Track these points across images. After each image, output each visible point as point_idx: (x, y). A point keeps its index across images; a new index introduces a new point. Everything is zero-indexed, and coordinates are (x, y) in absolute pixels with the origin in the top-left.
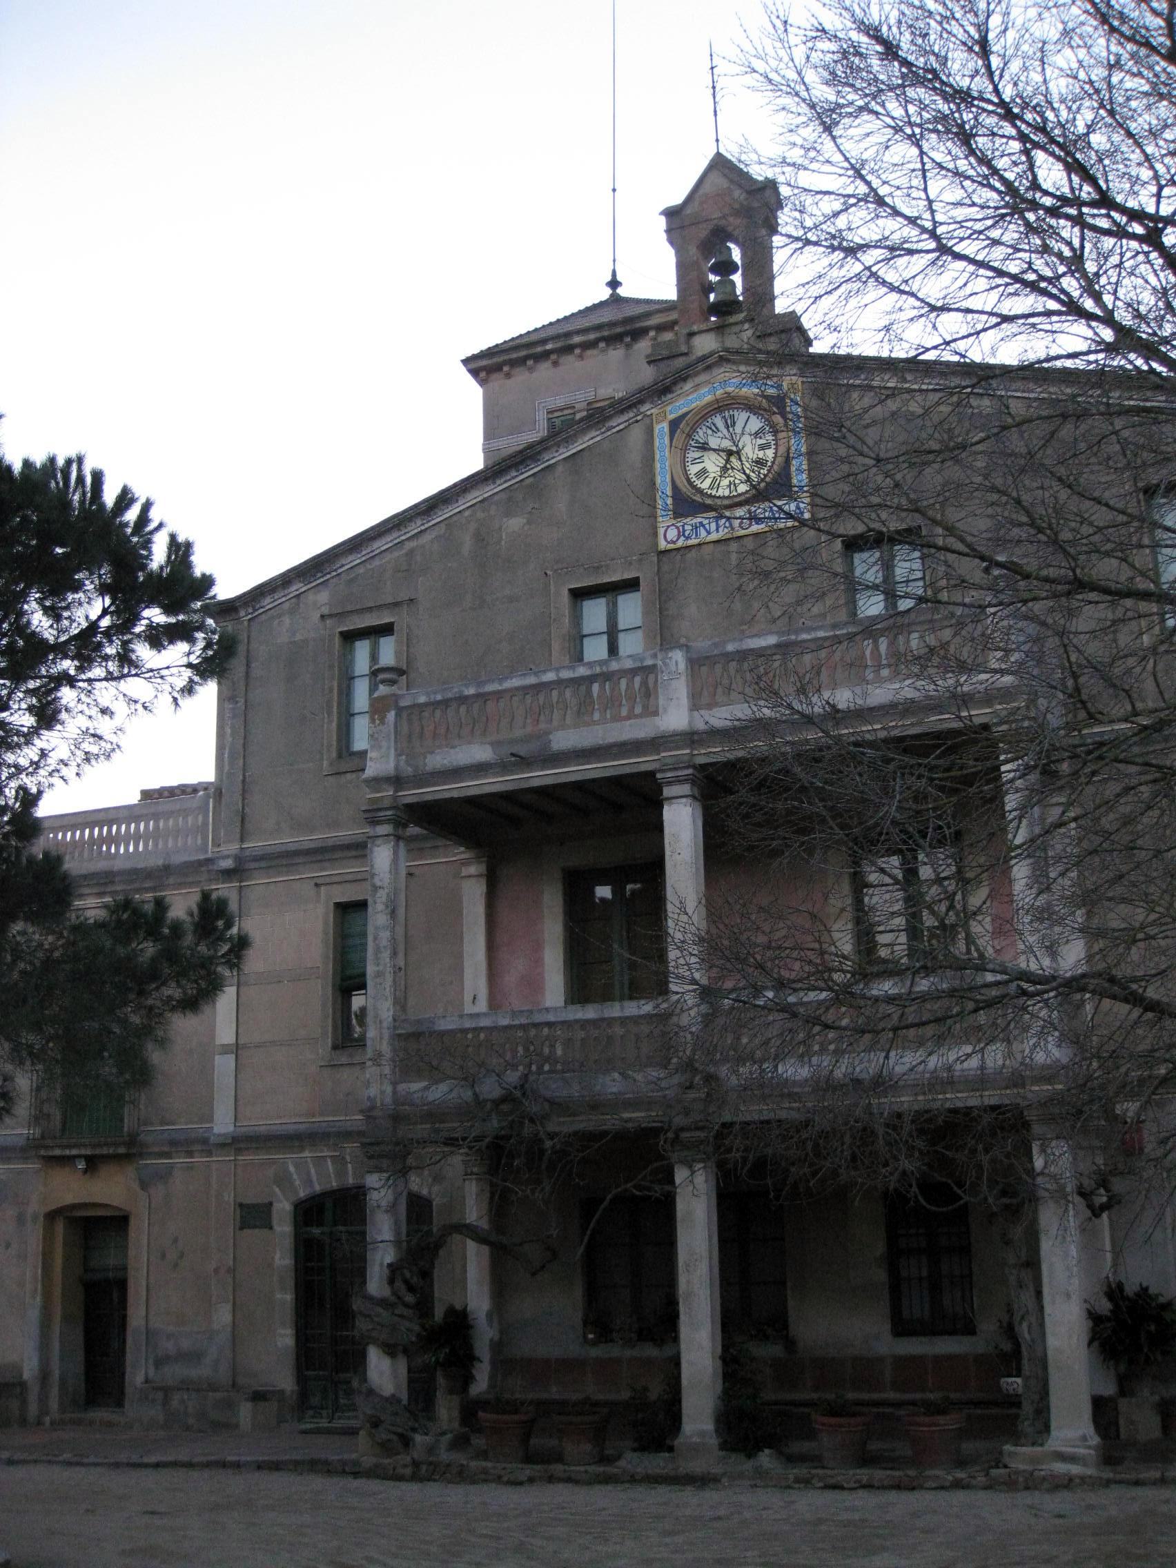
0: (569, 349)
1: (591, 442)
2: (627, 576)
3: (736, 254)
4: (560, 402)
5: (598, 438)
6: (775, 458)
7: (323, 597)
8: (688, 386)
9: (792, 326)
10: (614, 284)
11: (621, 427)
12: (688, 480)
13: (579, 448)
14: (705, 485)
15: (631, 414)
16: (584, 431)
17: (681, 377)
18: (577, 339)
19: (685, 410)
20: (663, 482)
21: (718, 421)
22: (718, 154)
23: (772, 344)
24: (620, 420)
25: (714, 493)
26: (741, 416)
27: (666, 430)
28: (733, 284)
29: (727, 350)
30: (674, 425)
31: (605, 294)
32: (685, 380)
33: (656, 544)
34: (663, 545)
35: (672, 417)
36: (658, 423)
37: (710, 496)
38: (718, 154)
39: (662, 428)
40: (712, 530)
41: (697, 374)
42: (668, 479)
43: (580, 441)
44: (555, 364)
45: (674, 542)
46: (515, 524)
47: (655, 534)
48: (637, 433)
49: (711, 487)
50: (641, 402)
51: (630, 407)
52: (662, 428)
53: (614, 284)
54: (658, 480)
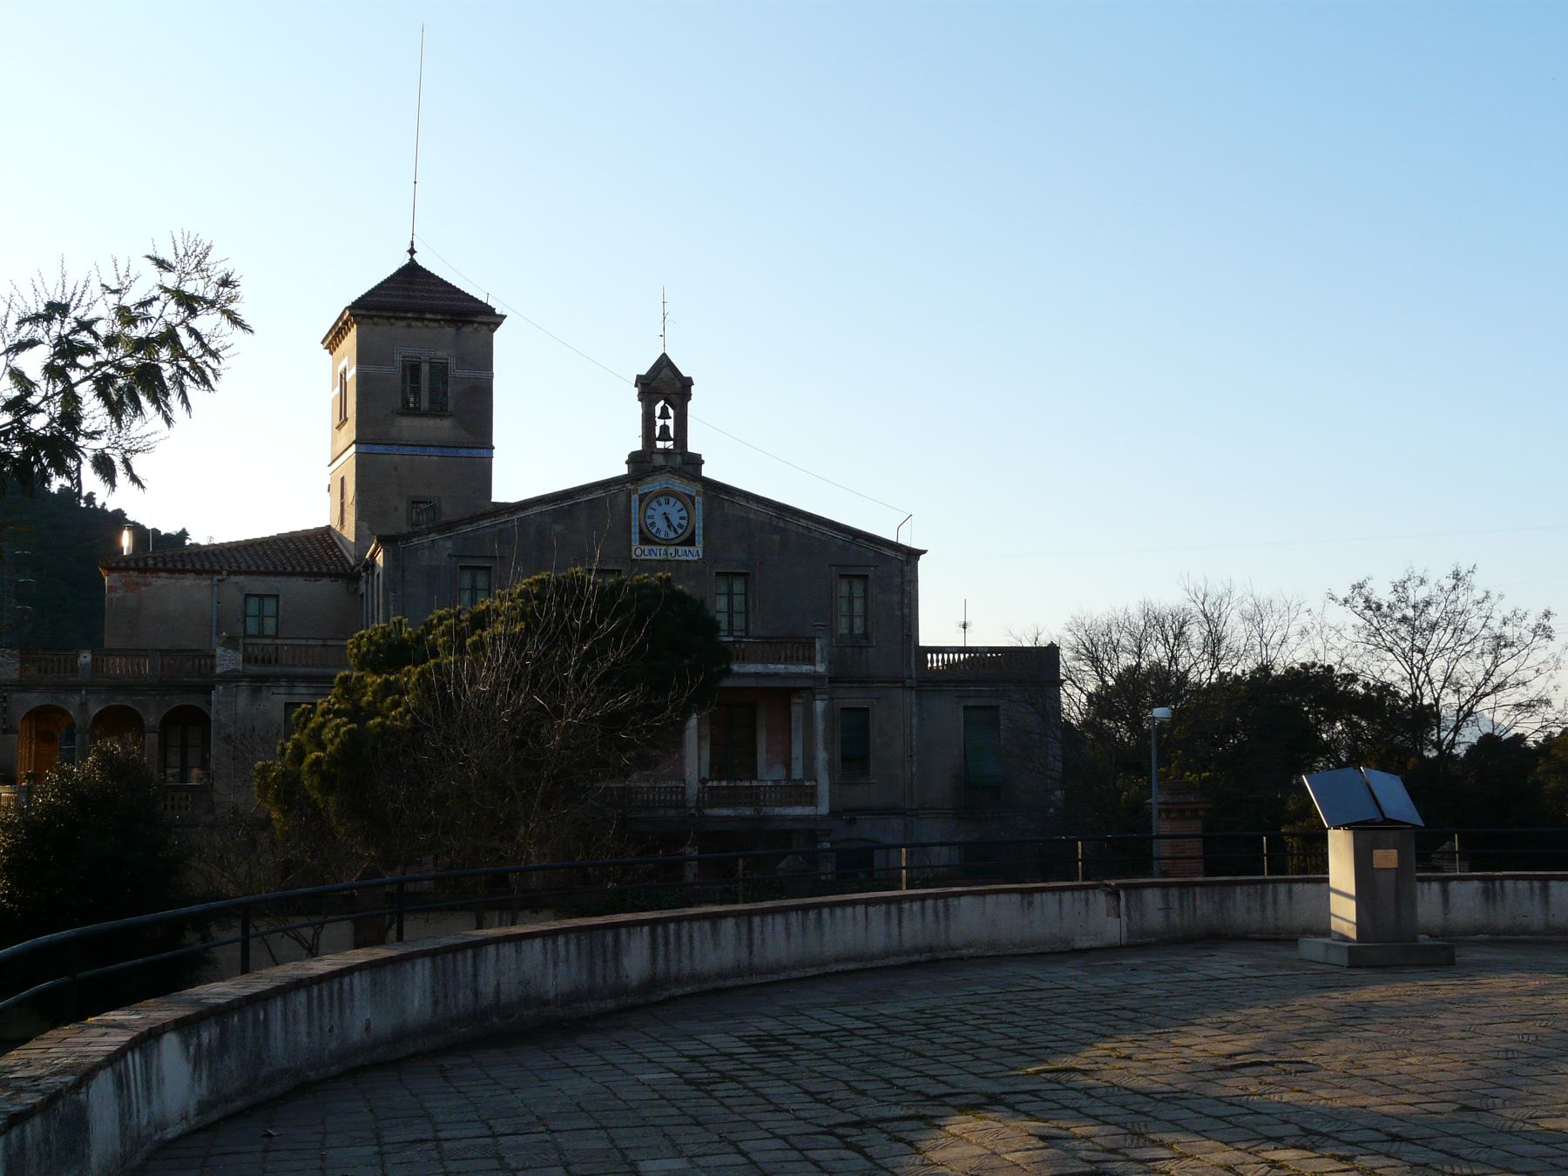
0: (422, 320)
3: (671, 412)
4: (410, 352)
7: (449, 544)
9: (697, 461)
10: (412, 252)
18: (428, 316)
20: (635, 524)
21: (662, 500)
23: (690, 469)
26: (672, 500)
31: (404, 260)
39: (635, 497)
40: (658, 553)
44: (409, 326)
46: (558, 528)
48: (622, 498)
52: (635, 497)
53: (412, 252)
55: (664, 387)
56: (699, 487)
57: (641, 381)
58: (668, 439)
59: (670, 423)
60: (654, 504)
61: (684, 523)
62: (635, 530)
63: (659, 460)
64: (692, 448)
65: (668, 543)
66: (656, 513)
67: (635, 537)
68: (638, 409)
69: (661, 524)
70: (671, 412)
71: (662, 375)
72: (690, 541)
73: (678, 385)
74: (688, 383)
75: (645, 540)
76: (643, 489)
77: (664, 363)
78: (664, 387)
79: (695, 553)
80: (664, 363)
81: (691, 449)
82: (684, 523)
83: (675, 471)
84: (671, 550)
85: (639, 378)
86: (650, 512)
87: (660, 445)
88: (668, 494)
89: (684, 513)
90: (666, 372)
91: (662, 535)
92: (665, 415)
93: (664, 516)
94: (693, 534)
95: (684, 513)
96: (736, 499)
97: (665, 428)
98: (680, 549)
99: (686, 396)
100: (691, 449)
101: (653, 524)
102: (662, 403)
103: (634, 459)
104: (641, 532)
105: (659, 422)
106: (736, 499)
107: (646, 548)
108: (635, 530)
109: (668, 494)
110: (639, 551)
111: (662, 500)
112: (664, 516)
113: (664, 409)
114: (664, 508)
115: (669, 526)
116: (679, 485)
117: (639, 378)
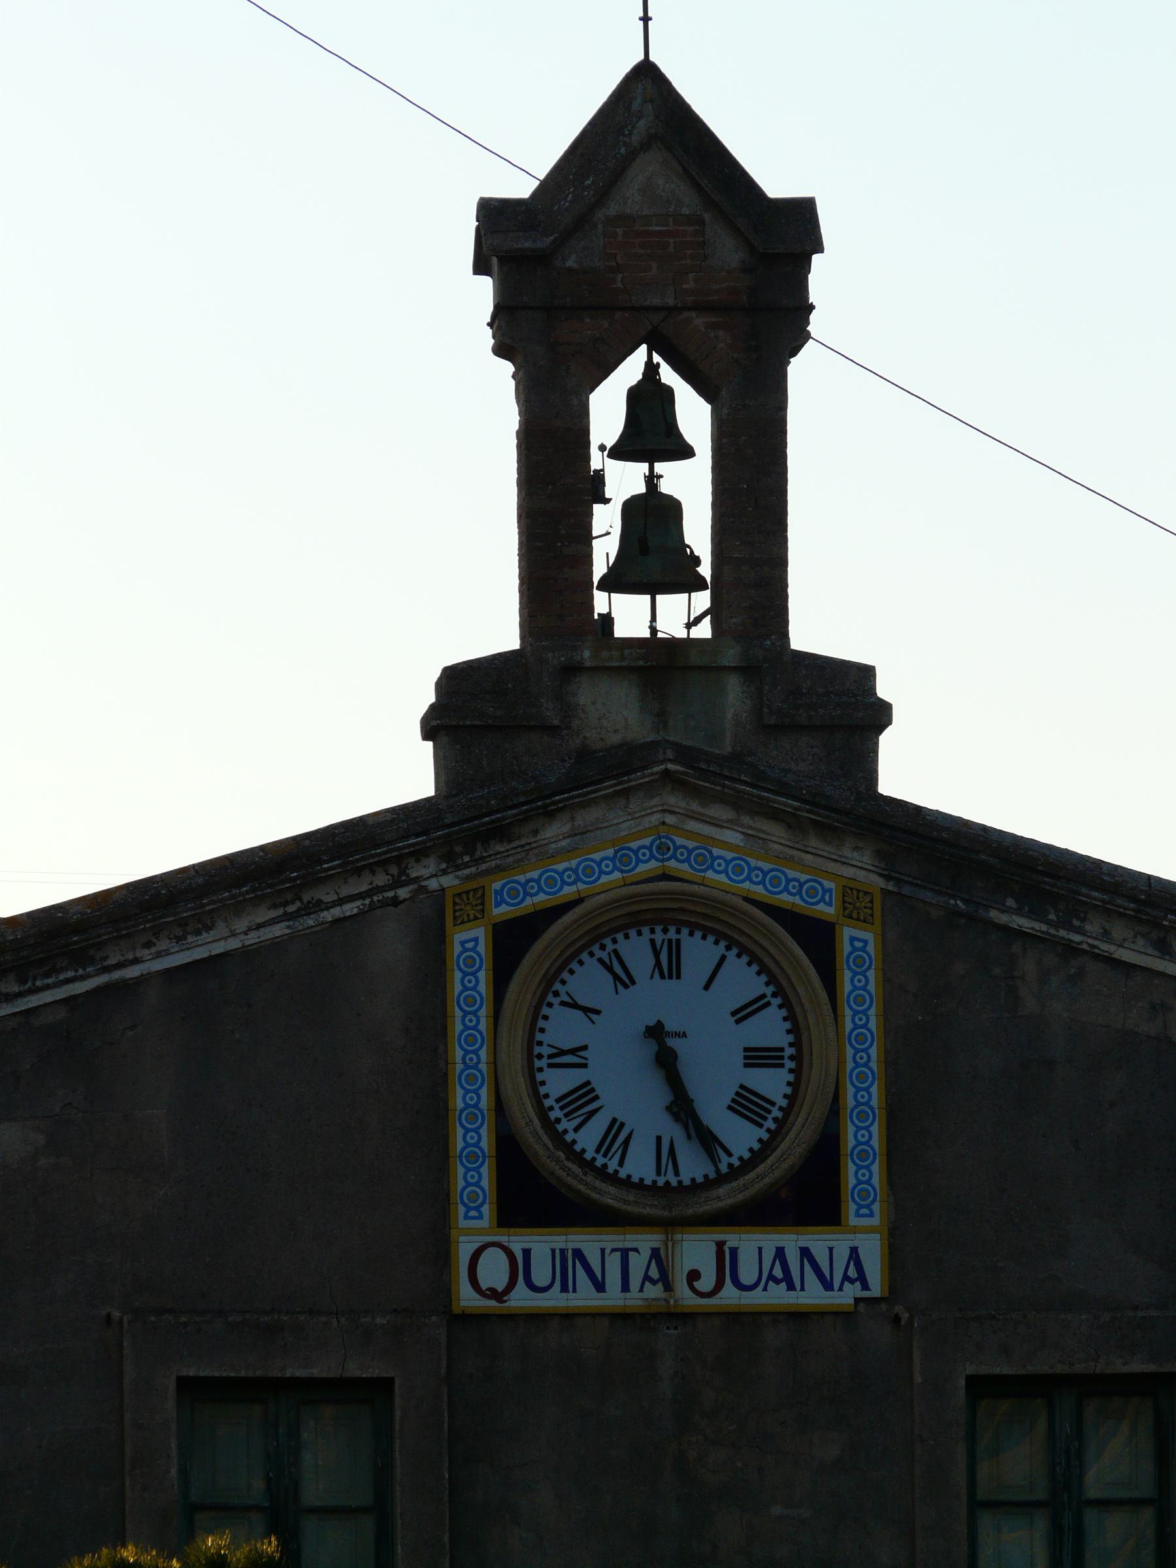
1: (252, 938)
2: (354, 1370)
3: (694, 415)
5: (278, 930)
6: (791, 1098)
8: (554, 832)
9: (848, 705)
11: (350, 909)
12: (543, 1113)
13: (219, 948)
14: (588, 1139)
15: (381, 879)
16: (238, 908)
17: (544, 804)
19: (541, 899)
20: (468, 1098)
22: (646, 80)
24: (345, 891)
25: (613, 1165)
26: (699, 953)
27: (483, 948)
28: (671, 510)
29: (685, 754)
30: (512, 941)
32: (550, 815)
33: (446, 1290)
34: (467, 1298)
35: (501, 912)
36: (459, 921)
37: (602, 1173)
38: (646, 80)
40: (599, 1274)
41: (583, 805)
42: (485, 1099)
43: (221, 929)
45: (493, 1294)
47: (444, 1257)
48: (391, 946)
49: (604, 1146)
50: (419, 854)
51: (383, 864)
52: (470, 942)
54: (458, 1099)
55: (649, 262)
56: (859, 865)
57: (505, 238)
58: (683, 578)
59: (690, 483)
60: (588, 981)
61: (772, 1084)
62: (472, 1140)
63: (612, 713)
64: (817, 625)
65: (671, 1208)
66: (601, 1032)
67: (474, 1179)
68: (491, 398)
69: (629, 1095)
70: (694, 415)
71: (630, 197)
72: (809, 1195)
73: (727, 252)
74: (792, 231)
75: (531, 1194)
76: (521, 890)
77: (647, 121)
78: (649, 262)
79: (853, 1252)
80: (647, 121)
81: (812, 629)
82: (772, 1084)
83: (704, 775)
84: (696, 1251)
85: (494, 216)
86: (562, 1027)
87: (629, 615)
88: (668, 913)
89: (770, 1028)
90: (652, 182)
91: (640, 1165)
92: (650, 432)
93: (661, 1049)
94: (826, 1154)
95: (770, 1028)
96: (1088, 935)
97: (653, 515)
98: (753, 1246)
99: (782, 320)
100: (812, 629)
101: (583, 1099)
102: (631, 369)
103: (466, 705)
104: (509, 1150)
105: (624, 480)
106: (1088, 935)
107: (541, 1246)
108: (472, 1140)
109: (668, 913)
110: (493, 1263)
111: (636, 951)
112: (661, 1049)
113: (649, 402)
114: (653, 999)
115: (682, 1107)
116: (733, 858)
117: (494, 216)
